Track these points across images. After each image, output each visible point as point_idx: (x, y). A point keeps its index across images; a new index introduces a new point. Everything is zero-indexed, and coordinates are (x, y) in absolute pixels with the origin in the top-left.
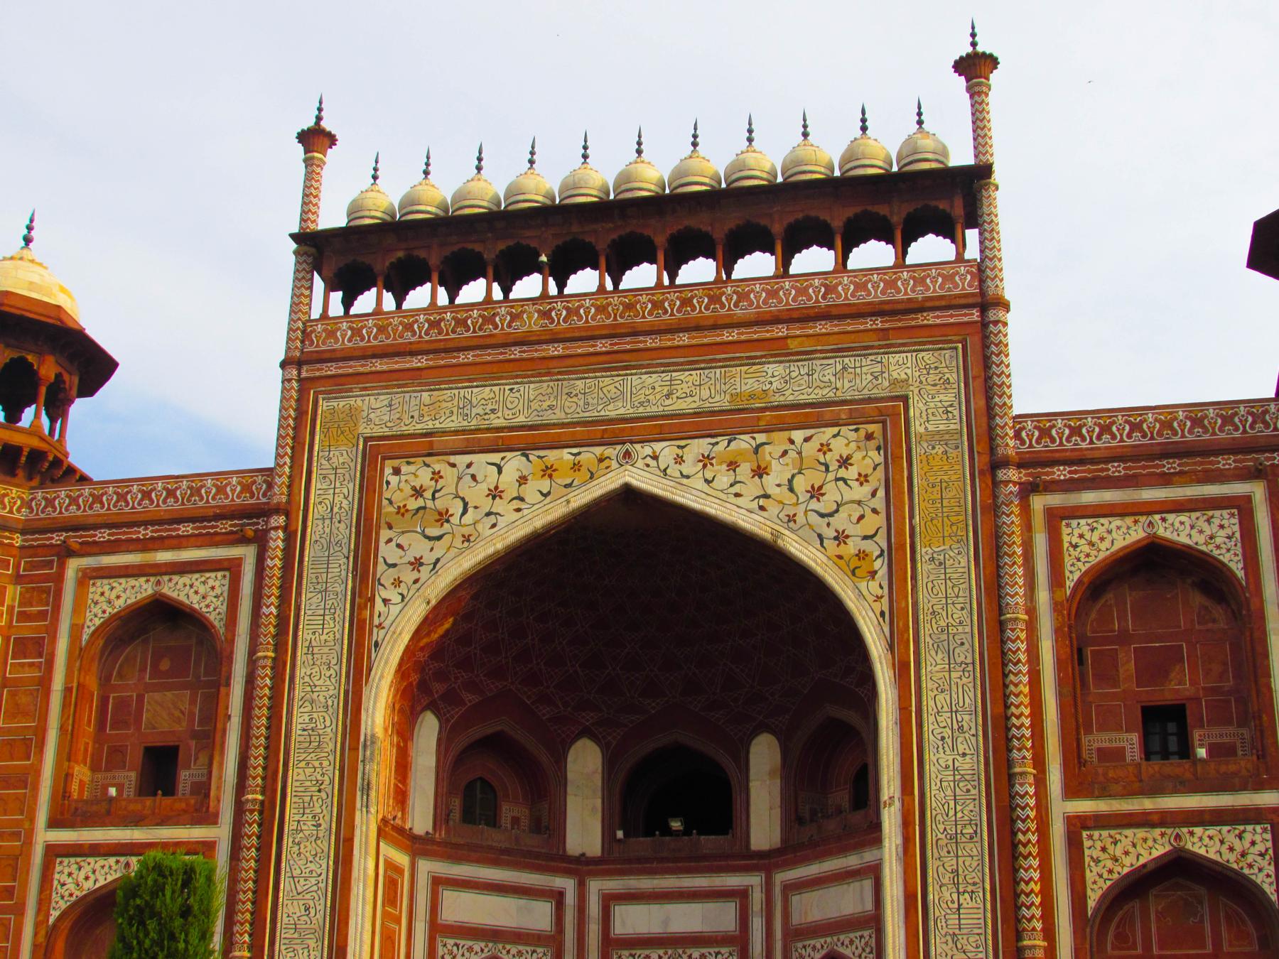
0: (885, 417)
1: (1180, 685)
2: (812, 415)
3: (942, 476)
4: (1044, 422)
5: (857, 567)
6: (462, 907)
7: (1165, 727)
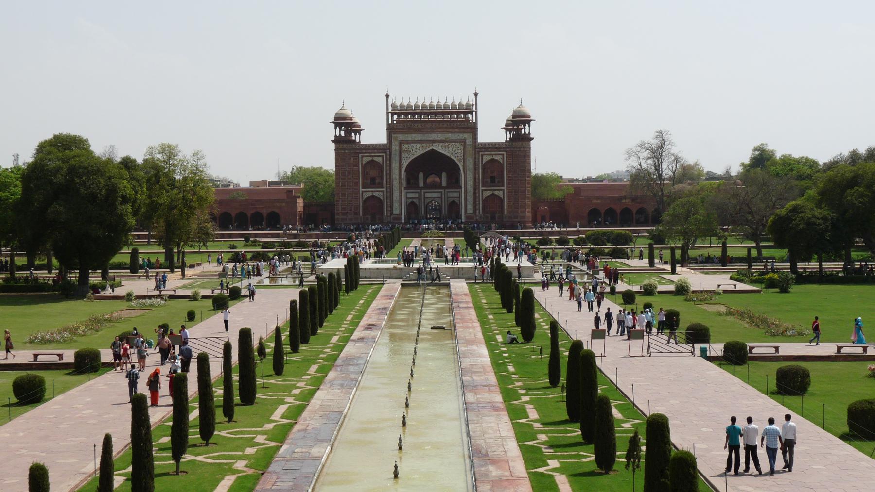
0: (463, 142)
1: (495, 174)
2: (455, 141)
3: (470, 149)
4: (481, 144)
5: (460, 160)
6: (410, 195)
7: (493, 179)
